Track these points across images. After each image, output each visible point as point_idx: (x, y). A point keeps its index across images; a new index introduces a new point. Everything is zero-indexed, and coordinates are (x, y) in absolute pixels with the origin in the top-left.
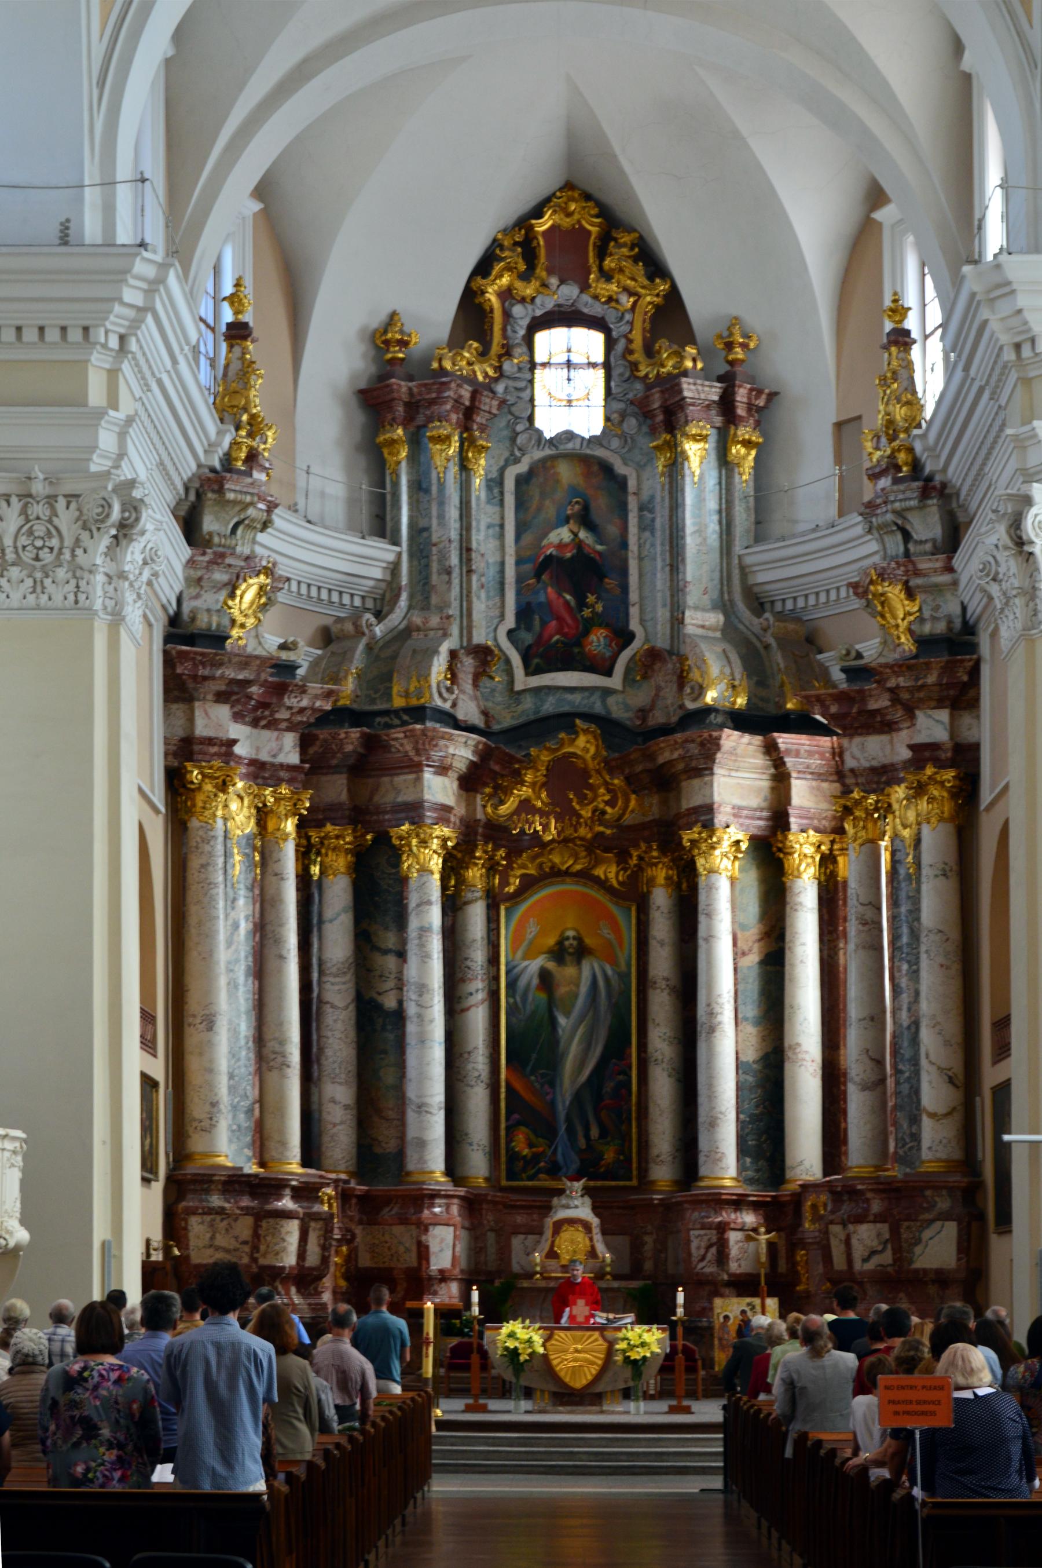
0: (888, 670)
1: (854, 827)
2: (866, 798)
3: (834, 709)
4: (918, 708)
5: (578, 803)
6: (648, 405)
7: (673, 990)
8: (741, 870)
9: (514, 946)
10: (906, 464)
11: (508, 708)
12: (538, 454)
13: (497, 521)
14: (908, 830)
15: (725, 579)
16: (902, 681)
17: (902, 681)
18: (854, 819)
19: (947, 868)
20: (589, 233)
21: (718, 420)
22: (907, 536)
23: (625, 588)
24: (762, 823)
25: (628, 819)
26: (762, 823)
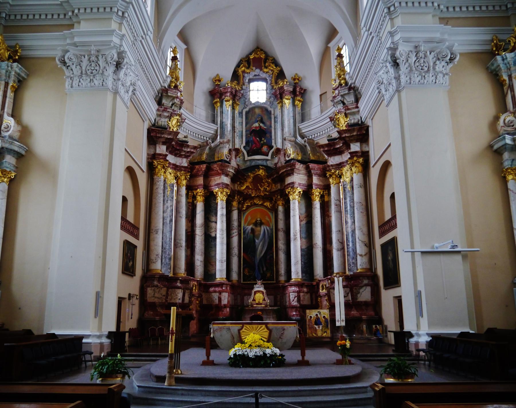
0: (343, 132)
1: (333, 180)
2: (335, 172)
3: (326, 149)
4: (351, 143)
5: (260, 187)
6: (276, 93)
7: (284, 231)
8: (301, 200)
9: (245, 223)
10: (343, 83)
11: (244, 164)
12: (251, 106)
13: (241, 121)
14: (348, 179)
15: (295, 132)
16: (347, 135)
17: (347, 135)
18: (332, 178)
19: (361, 185)
20: (262, 58)
21: (292, 96)
22: (344, 103)
23: (271, 137)
24: (306, 187)
25: (273, 190)
26: (306, 187)
